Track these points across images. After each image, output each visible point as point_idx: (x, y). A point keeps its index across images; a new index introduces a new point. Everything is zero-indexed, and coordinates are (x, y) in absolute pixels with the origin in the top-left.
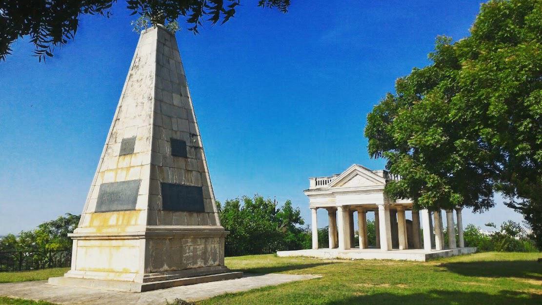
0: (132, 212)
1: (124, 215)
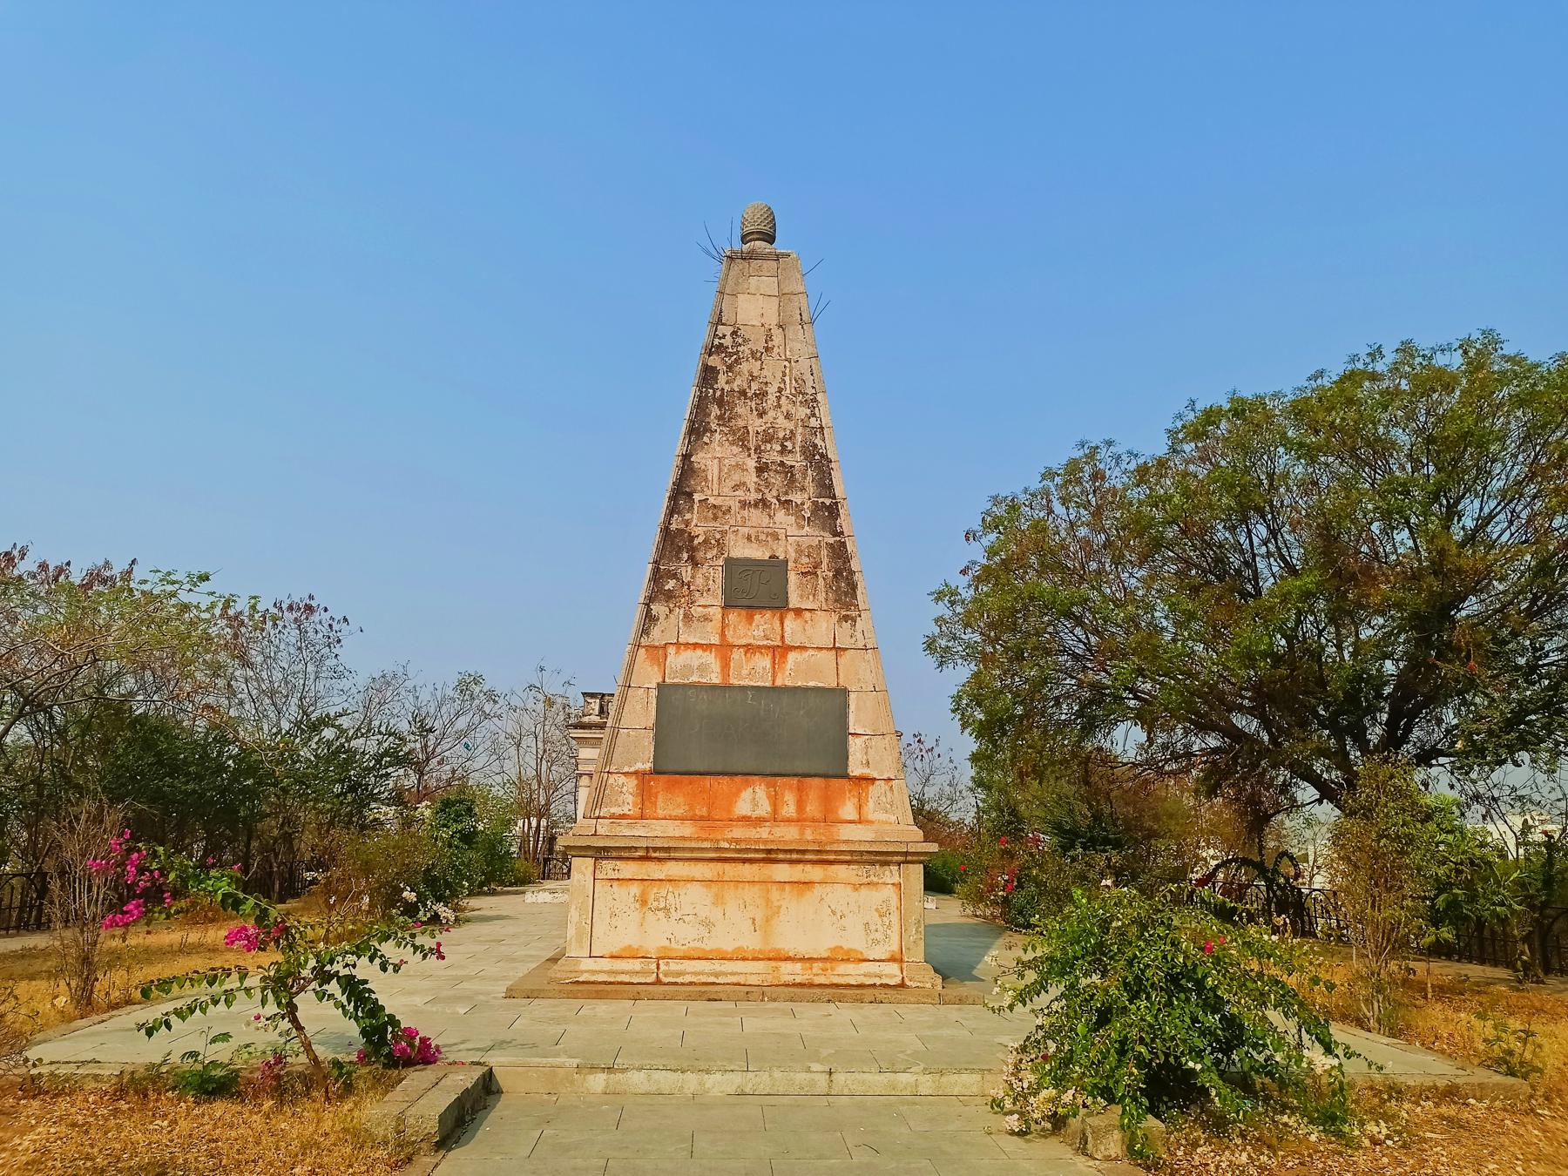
0: (836, 783)
1: (800, 790)
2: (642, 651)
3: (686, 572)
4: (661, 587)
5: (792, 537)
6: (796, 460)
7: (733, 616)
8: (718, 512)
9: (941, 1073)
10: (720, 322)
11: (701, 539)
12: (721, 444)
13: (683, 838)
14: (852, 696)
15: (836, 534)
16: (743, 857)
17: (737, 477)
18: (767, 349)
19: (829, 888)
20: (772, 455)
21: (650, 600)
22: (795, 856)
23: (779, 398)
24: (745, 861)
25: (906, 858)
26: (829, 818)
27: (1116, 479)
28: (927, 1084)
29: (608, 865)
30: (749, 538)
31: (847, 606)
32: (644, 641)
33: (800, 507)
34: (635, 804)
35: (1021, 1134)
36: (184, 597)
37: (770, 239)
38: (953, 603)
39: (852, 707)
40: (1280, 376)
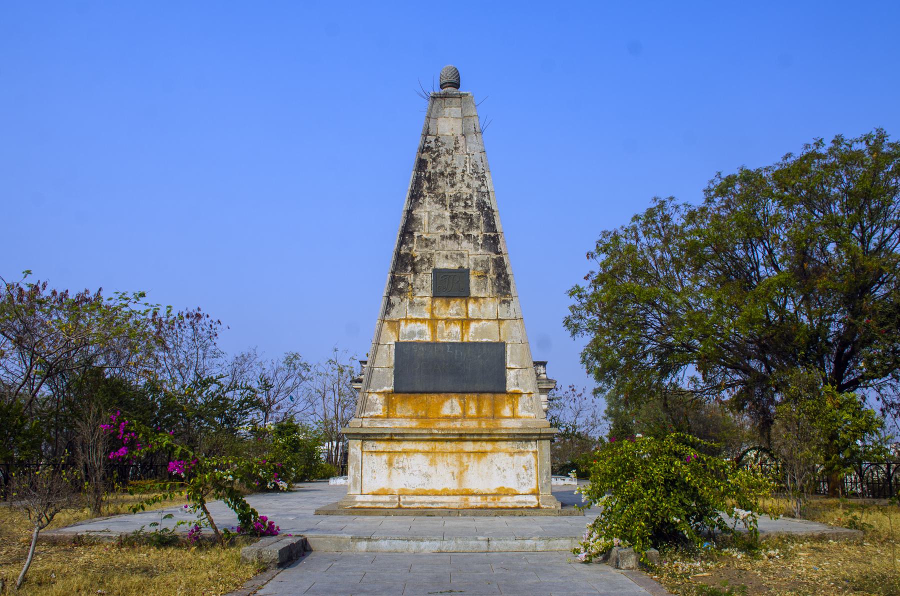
0: (499, 396)
1: (478, 400)
2: (386, 324)
3: (410, 278)
4: (396, 287)
5: (472, 255)
6: (474, 211)
7: (438, 302)
8: (428, 243)
9: (549, 539)
10: (428, 134)
11: (418, 258)
12: (429, 203)
13: (412, 428)
14: (509, 347)
15: (497, 253)
16: (446, 438)
17: (439, 222)
18: (456, 148)
19: (496, 455)
20: (460, 209)
21: (390, 294)
22: (476, 437)
23: (463, 176)
24: (447, 440)
25: (540, 437)
26: (495, 415)
27: (677, 220)
28: (541, 545)
29: (369, 445)
30: (447, 257)
31: (505, 295)
32: (387, 318)
33: (476, 238)
34: (384, 410)
35: (586, 562)
36: (132, 306)
37: (457, 85)
38: (580, 297)
39: (508, 353)
40: (767, 156)
